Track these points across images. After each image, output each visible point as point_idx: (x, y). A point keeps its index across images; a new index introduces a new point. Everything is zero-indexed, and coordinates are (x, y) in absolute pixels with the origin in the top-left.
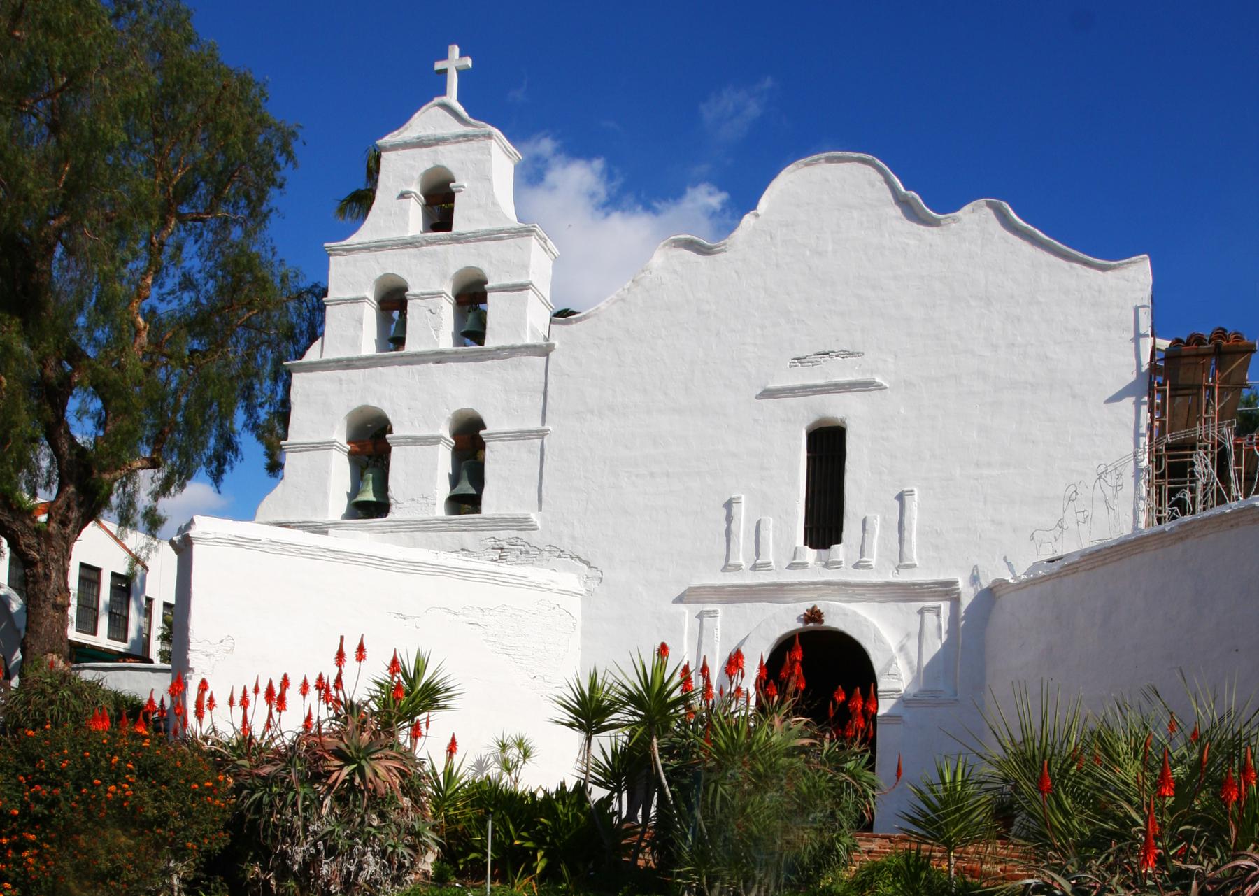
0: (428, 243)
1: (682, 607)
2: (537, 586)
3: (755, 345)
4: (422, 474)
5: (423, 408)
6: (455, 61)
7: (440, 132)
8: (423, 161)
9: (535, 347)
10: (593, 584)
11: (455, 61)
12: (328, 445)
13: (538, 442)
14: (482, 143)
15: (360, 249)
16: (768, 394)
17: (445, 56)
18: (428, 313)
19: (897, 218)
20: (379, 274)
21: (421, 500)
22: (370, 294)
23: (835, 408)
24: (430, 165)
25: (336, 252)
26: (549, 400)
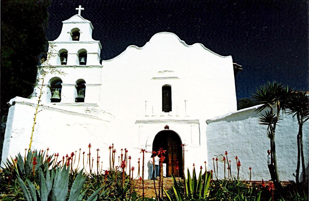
4: (69, 92)
5: (69, 77)
6: (80, 8)
11: (80, 8)
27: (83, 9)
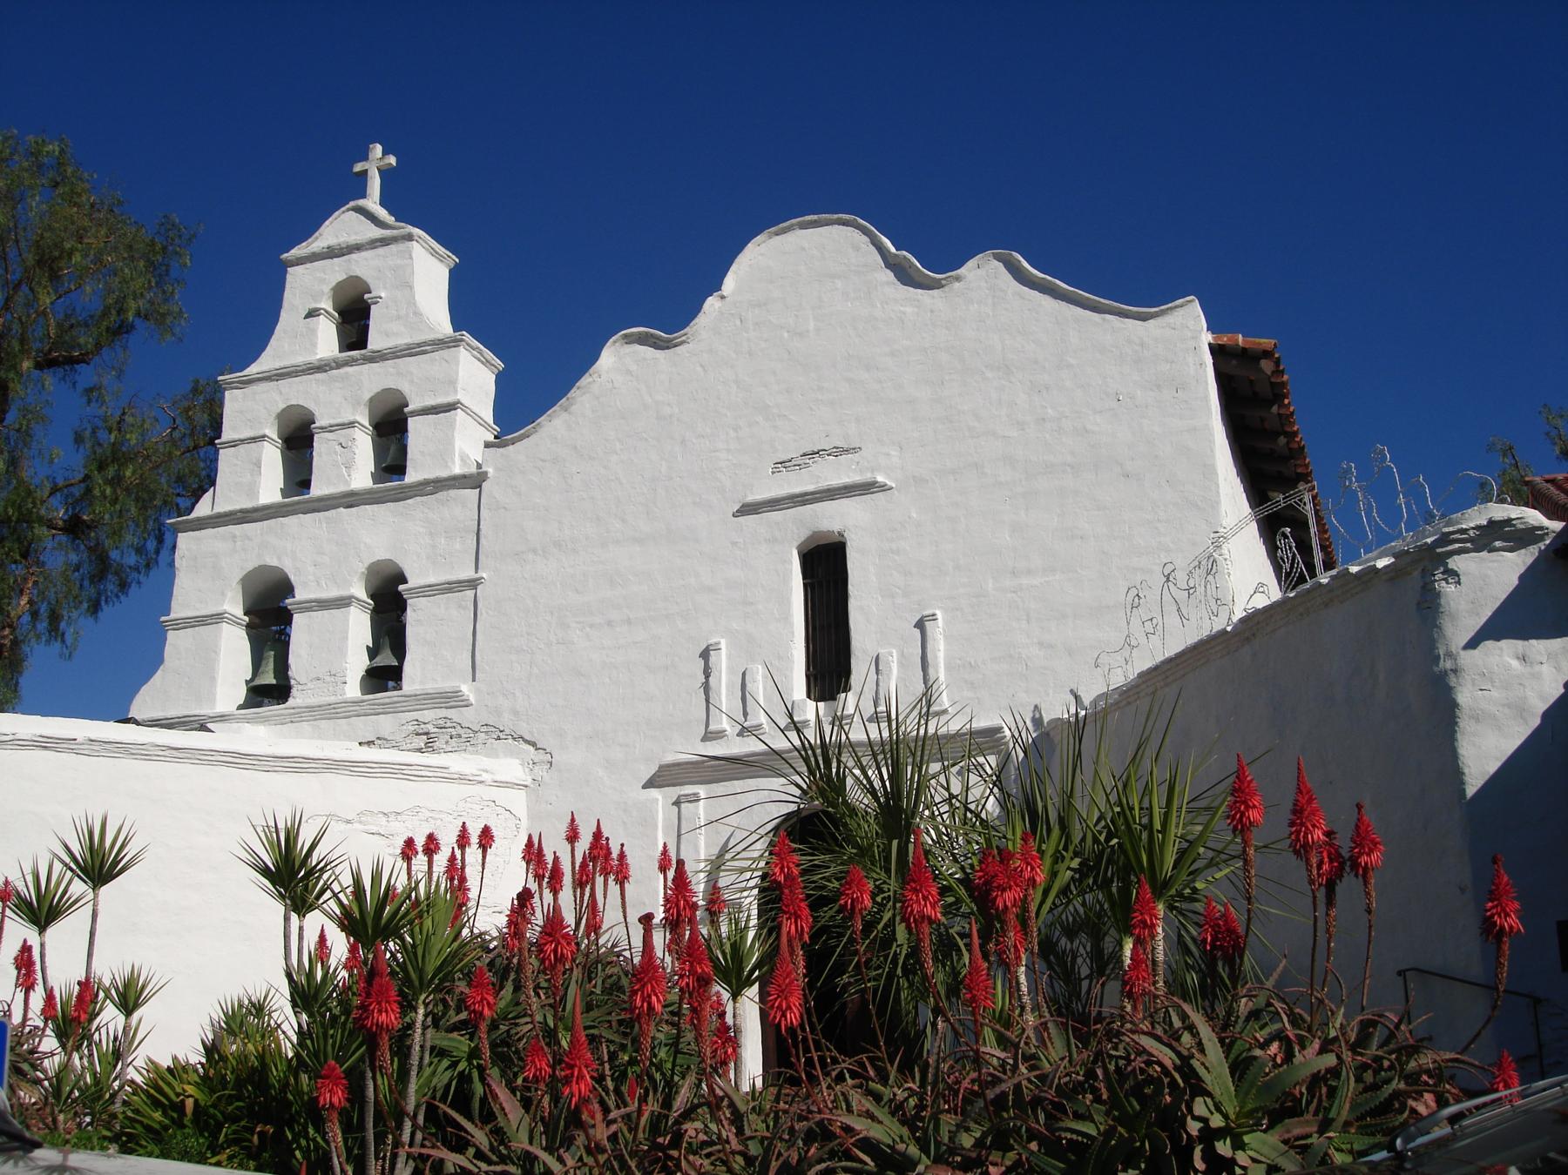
0: (347, 363)
1: (654, 793)
2: (462, 779)
3: (728, 451)
4: (332, 646)
5: (327, 560)
7: (353, 239)
8: (334, 272)
9: (464, 477)
10: (540, 771)
12: (217, 618)
13: (470, 593)
14: (402, 246)
15: (259, 380)
16: (748, 509)
17: (365, 157)
18: (338, 448)
19: (888, 283)
20: (282, 406)
21: (328, 679)
22: (272, 432)
23: (831, 518)
24: (341, 277)
25: (233, 386)
26: (482, 541)
27: (392, 160)
